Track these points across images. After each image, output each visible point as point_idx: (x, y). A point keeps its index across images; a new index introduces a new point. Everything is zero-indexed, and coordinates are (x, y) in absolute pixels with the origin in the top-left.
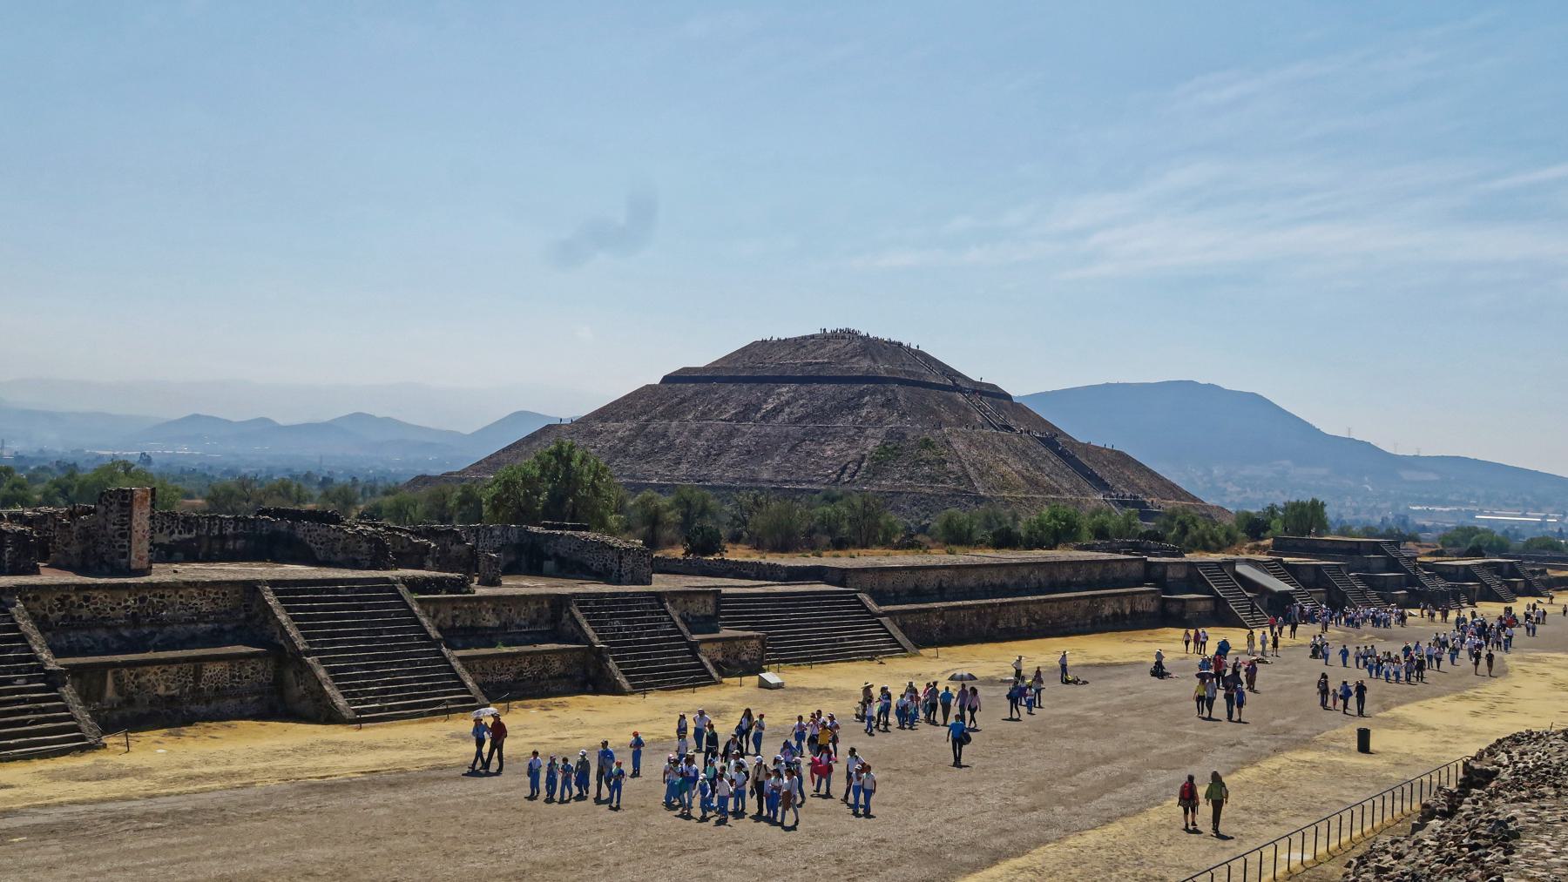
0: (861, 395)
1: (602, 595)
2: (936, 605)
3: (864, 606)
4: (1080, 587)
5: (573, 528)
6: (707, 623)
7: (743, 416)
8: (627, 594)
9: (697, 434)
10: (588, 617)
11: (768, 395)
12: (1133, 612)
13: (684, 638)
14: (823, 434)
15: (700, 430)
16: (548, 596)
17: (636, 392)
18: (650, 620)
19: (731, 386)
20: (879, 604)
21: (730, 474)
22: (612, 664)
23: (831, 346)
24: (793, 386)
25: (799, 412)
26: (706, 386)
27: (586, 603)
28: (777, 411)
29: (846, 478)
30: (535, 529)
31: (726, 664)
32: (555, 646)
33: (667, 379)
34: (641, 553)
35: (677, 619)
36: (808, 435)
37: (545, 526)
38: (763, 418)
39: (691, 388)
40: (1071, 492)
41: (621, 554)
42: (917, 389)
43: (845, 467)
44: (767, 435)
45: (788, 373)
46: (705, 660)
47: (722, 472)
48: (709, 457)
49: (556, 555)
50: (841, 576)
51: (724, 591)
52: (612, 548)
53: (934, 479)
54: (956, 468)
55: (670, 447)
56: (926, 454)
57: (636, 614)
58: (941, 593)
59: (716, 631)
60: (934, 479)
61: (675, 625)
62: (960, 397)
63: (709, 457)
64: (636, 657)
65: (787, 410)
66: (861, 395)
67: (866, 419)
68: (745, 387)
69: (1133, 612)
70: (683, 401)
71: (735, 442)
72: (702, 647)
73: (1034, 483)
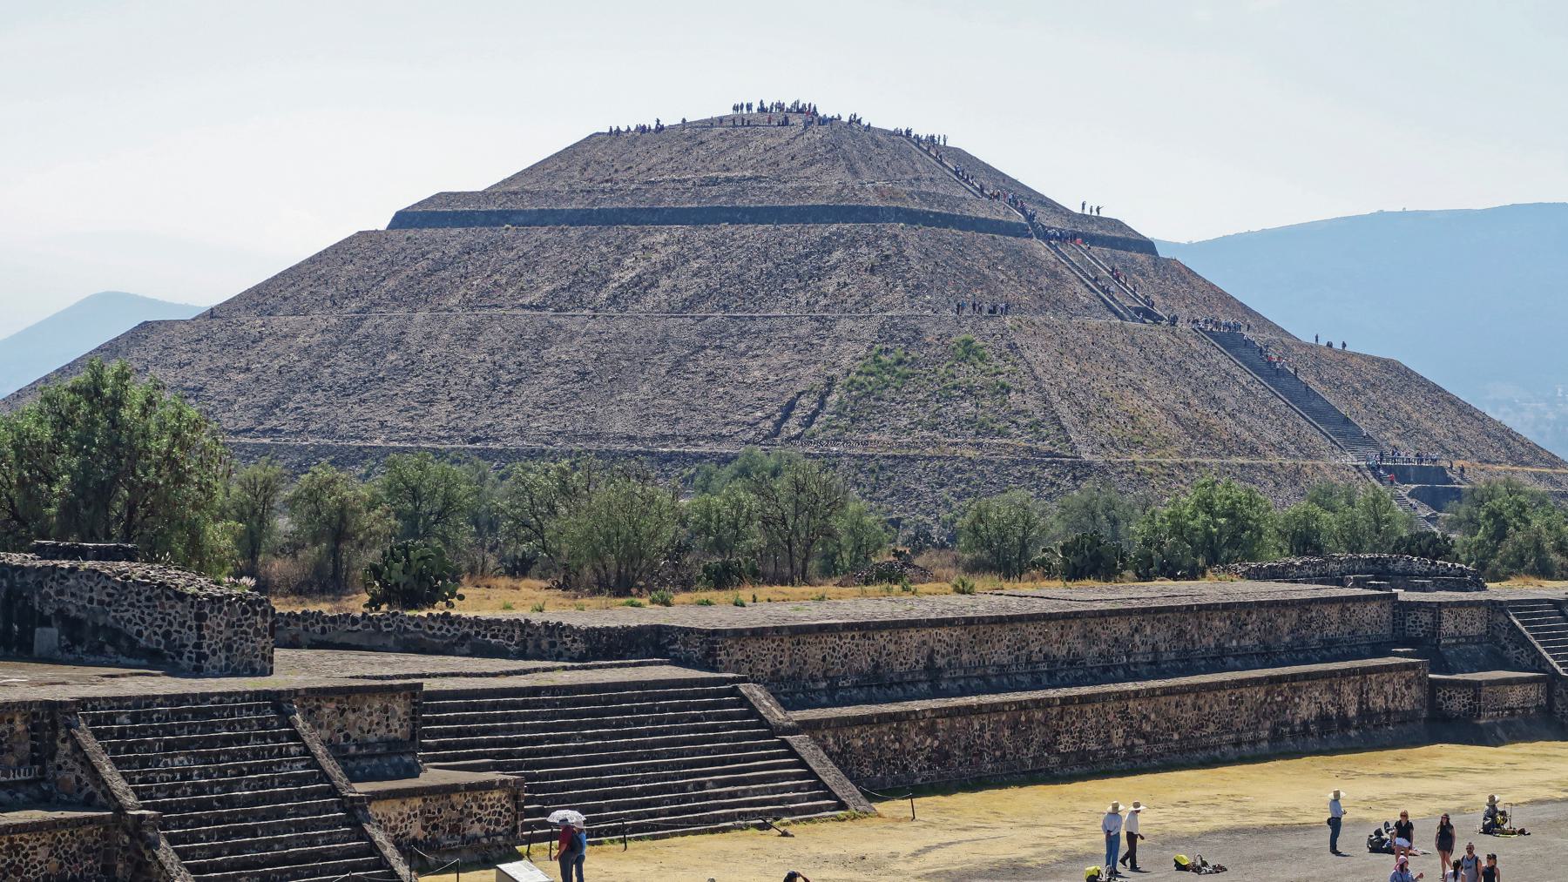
0: (826, 246)
1: (150, 700)
2: (917, 705)
3: (753, 712)
4: (1247, 659)
5: (102, 555)
6: (395, 757)
7: (570, 296)
8: (205, 697)
9: (470, 338)
10: (115, 750)
12: (1366, 713)
13: (333, 791)
14: (743, 334)
15: (477, 329)
16: (24, 705)
17: (336, 249)
18: (256, 754)
19: (541, 233)
20: (787, 706)
21: (542, 424)
22: (166, 853)
23: (759, 142)
24: (679, 231)
25: (695, 286)
26: (487, 232)
27: (111, 719)
28: (641, 285)
29: (792, 427)
30: (16, 559)
31: (431, 846)
32: (37, 815)
33: (402, 220)
34: (250, 606)
35: (319, 750)
36: (710, 338)
37: (41, 551)
38: (613, 299)
39: (456, 238)
40: (1281, 449)
41: (200, 608)
42: (950, 233)
43: (791, 406)
44: (622, 337)
45: (668, 202)
46: (380, 837)
47: (519, 420)
48: (494, 387)
49: (61, 614)
50: (706, 647)
51: (429, 685)
52: (181, 596)
53: (984, 429)
54: (1031, 403)
55: (411, 368)
56: (967, 374)
57: (227, 741)
58: (933, 679)
59: (412, 772)
60: (984, 429)
61: (314, 762)
62: (1039, 247)
63: (494, 387)
64: (224, 835)
65: (665, 283)
66: (826, 246)
67: (837, 301)
68: (574, 233)
69: (1366, 713)
70: (440, 266)
71: (551, 353)
72: (376, 809)
73: (1201, 433)
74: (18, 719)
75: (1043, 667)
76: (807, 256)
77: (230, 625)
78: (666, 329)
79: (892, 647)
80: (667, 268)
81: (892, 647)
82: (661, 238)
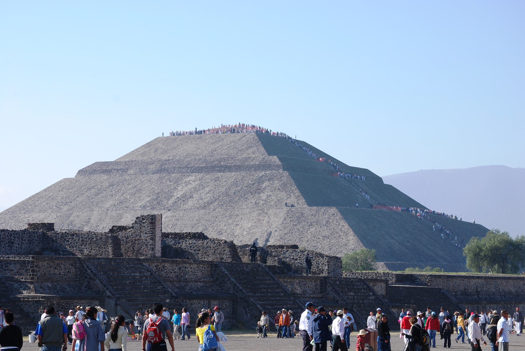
0: (260, 180)
11: (177, 182)
24: (200, 175)
25: (207, 198)
33: (81, 172)
66: (260, 180)
74: (318, 281)
75: (503, 294)
76: (254, 184)
77: (334, 265)
79: (468, 284)
81: (468, 284)
82: (191, 178)
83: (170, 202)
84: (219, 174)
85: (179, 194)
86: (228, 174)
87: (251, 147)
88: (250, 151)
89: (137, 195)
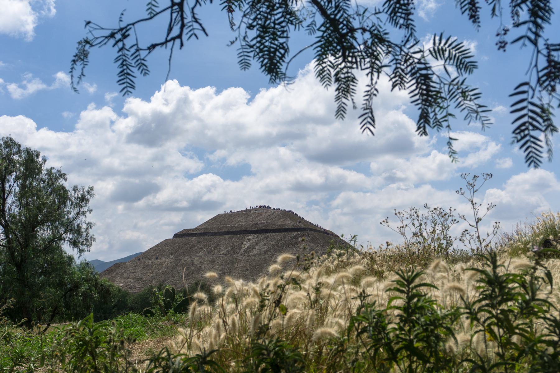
24: (256, 235)
28: (251, 248)
33: (176, 236)
38: (245, 252)
65: (257, 247)
66: (296, 237)
78: (264, 258)
80: (257, 244)
83: (242, 251)
84: (268, 234)
85: (246, 246)
86: (274, 234)
87: (281, 219)
88: (281, 220)
89: (219, 247)
